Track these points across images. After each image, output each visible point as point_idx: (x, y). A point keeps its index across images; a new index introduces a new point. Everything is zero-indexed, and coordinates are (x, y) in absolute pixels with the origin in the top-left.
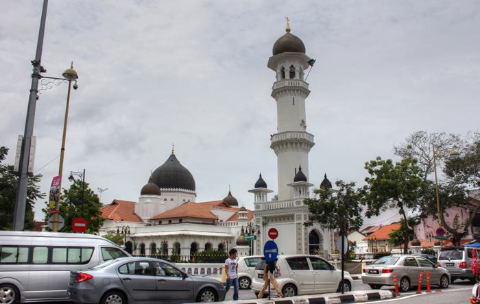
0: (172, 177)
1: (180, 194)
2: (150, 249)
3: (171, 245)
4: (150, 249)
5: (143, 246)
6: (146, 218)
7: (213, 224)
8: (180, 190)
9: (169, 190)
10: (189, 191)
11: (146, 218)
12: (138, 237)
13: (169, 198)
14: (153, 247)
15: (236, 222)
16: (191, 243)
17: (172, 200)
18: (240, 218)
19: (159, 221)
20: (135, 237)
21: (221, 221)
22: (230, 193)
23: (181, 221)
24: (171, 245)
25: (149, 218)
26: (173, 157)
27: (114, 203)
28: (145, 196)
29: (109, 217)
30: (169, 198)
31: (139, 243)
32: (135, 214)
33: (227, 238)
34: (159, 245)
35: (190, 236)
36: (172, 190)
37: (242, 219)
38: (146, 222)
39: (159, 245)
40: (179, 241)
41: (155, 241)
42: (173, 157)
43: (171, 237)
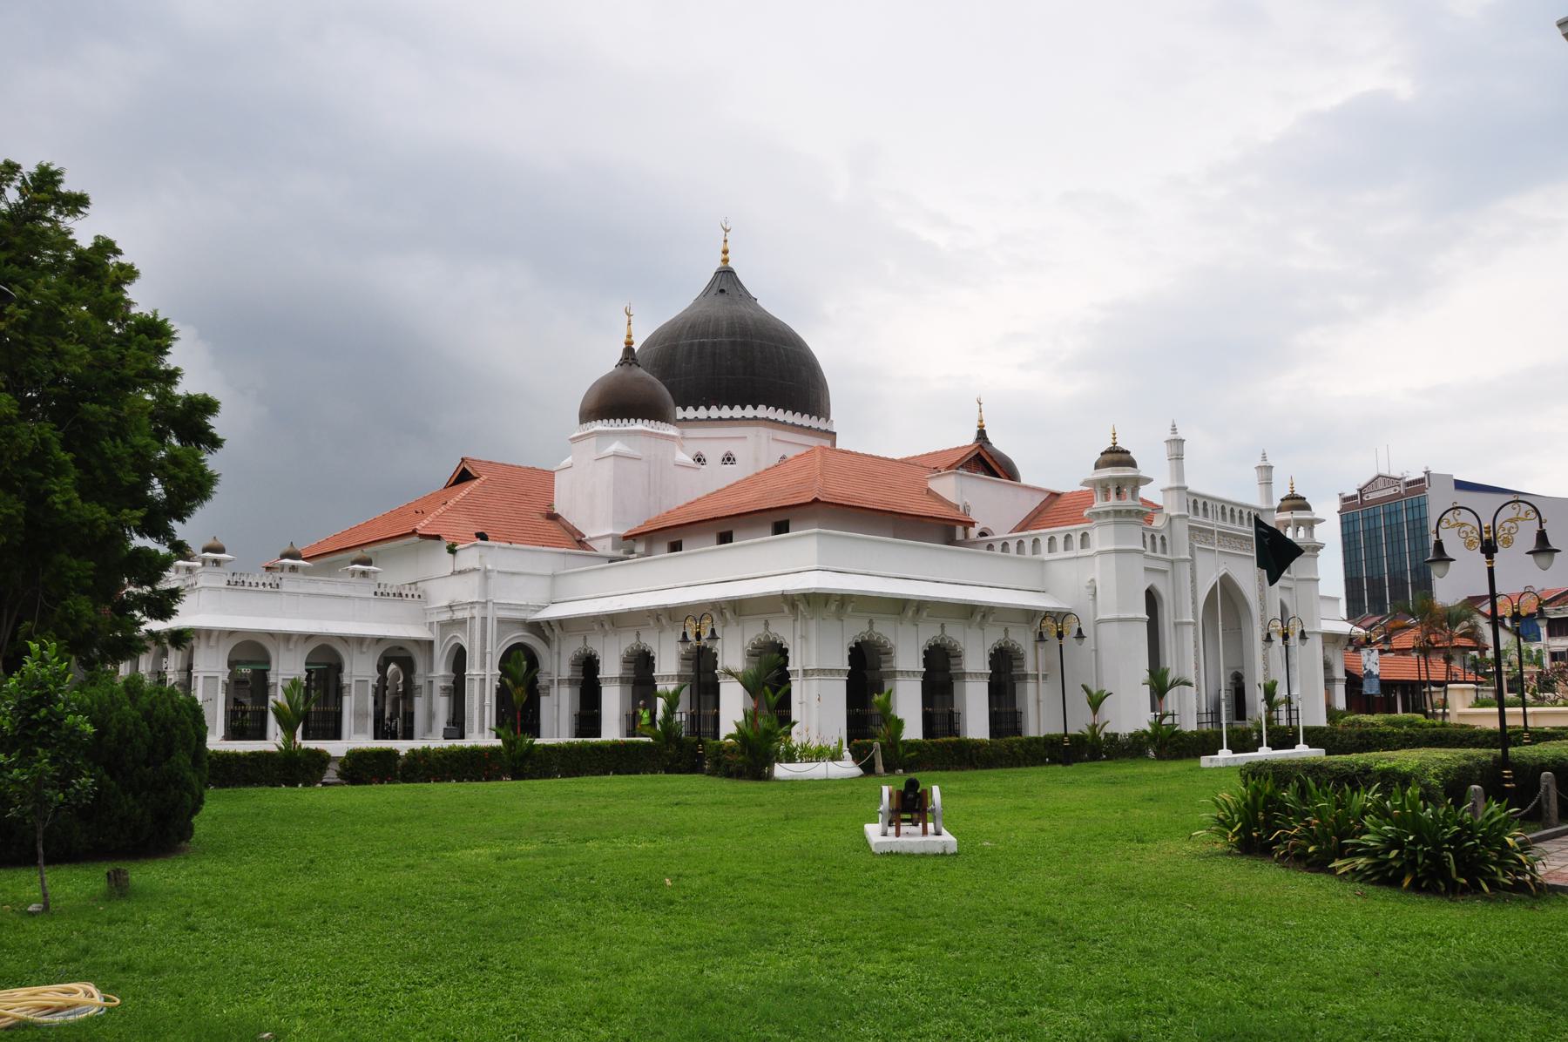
0: (733, 361)
1: (764, 432)
2: (623, 680)
3: (732, 655)
4: (623, 680)
5: (588, 667)
6: (600, 527)
7: (950, 540)
8: (762, 411)
9: (714, 412)
10: (805, 421)
11: (600, 527)
12: (562, 623)
13: (714, 452)
14: (641, 667)
15: (1076, 530)
16: (848, 641)
17: (729, 459)
18: (1099, 504)
19: (669, 536)
20: (548, 622)
21: (982, 534)
22: (982, 434)
23: (781, 528)
24: (732, 655)
25: (623, 532)
26: (726, 281)
27: (463, 476)
28: (599, 426)
29: (421, 527)
30: (714, 452)
31: (571, 648)
32: (553, 517)
33: (1030, 615)
34: (668, 665)
35: (842, 603)
36: (726, 412)
37: (1117, 513)
38: (605, 548)
39: (668, 665)
40: (784, 631)
41: (650, 641)
42: (726, 281)
43: (737, 608)
